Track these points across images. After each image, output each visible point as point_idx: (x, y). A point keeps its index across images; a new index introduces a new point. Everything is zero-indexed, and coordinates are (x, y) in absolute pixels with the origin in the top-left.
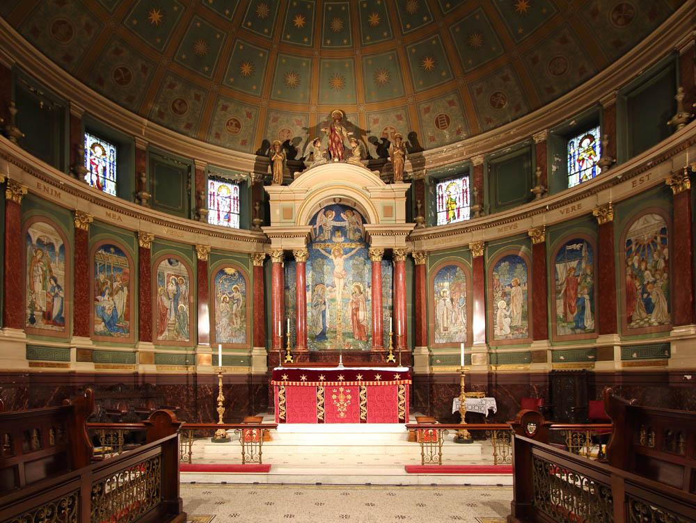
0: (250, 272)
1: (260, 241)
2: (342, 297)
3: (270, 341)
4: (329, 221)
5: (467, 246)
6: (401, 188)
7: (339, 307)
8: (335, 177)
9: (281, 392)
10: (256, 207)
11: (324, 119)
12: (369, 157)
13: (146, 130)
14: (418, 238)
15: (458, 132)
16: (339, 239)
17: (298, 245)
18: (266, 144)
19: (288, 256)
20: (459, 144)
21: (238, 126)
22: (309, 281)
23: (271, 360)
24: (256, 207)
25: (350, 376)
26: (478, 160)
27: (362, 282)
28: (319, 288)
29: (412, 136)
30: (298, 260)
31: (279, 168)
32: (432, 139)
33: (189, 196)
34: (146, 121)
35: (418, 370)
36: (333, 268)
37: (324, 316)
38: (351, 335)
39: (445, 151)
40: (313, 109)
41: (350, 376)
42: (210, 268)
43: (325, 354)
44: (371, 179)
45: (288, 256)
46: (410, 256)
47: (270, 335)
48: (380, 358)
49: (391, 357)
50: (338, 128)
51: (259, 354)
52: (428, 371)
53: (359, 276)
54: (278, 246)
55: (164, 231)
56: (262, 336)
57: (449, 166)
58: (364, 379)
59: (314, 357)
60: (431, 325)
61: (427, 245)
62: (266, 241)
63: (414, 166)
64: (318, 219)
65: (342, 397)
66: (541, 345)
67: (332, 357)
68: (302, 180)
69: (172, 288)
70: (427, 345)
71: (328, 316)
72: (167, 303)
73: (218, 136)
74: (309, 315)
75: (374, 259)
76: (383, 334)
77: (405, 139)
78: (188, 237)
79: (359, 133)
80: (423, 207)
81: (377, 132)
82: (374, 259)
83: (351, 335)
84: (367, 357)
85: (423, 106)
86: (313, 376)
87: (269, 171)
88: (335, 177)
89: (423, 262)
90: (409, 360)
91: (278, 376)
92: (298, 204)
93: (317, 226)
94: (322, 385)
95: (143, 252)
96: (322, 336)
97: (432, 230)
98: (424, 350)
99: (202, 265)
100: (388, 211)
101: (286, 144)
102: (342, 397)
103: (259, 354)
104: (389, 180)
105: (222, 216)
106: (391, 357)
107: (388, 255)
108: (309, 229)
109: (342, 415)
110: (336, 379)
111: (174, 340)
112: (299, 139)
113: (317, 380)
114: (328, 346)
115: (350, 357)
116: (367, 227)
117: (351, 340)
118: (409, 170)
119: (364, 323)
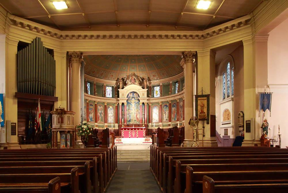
0: (115, 107)
1: (117, 100)
2: (134, 113)
3: (119, 122)
4: (131, 95)
5: (158, 102)
6: (146, 90)
7: (133, 114)
8: (133, 87)
9: (123, 132)
10: (116, 93)
11: (130, 74)
12: (140, 81)
13: (96, 80)
14: (150, 100)
15: (157, 78)
16: (133, 99)
17: (125, 102)
18: (118, 79)
19: (123, 104)
20: (158, 80)
21: (113, 76)
22: (127, 109)
23: (120, 126)
24: (116, 93)
25: (135, 129)
26: (161, 84)
27: (138, 109)
28: (129, 111)
29: (149, 78)
30: (125, 105)
31: (121, 86)
32: (153, 79)
33: (103, 91)
34: (96, 78)
35: (149, 128)
36: (132, 106)
37: (130, 116)
38: (136, 121)
39: (155, 81)
40: (128, 72)
41: (135, 129)
42: (107, 106)
43: (130, 125)
44: (140, 87)
45: (123, 104)
46: (148, 103)
47: (119, 120)
48: (141, 125)
49: (144, 125)
50: (133, 77)
51: (117, 125)
52: (151, 128)
53: (137, 108)
54: (121, 102)
55: (99, 100)
56: (117, 120)
57: (156, 84)
58: (137, 130)
59: (128, 125)
60: (152, 118)
61: (151, 101)
62: (118, 100)
63: (149, 83)
64: (129, 95)
65: (133, 133)
66: (170, 123)
67: (132, 125)
68: (126, 88)
69: (100, 112)
70: (151, 123)
71: (131, 116)
72: (100, 115)
73: (108, 78)
74: (127, 116)
75: (140, 105)
76: (142, 121)
77: (147, 78)
78: (103, 101)
79: (137, 77)
80: (151, 93)
81: (142, 76)
82: (140, 105)
83: (136, 121)
84: (139, 125)
85: (150, 73)
86: (128, 129)
87: (119, 84)
88: (133, 87)
89: (151, 105)
90: (147, 126)
91: (122, 129)
92: (125, 93)
93: (129, 97)
94: (130, 131)
95: (96, 105)
96: (130, 121)
97: (152, 98)
98: (150, 124)
99: (105, 106)
100: (143, 94)
101: (122, 79)
102: (133, 133)
103: (117, 125)
104: (143, 88)
105: (108, 94)
106: (144, 125)
107: (143, 103)
108: (127, 98)
109: (134, 136)
110: (133, 130)
111: (100, 122)
112: (125, 77)
113: (129, 130)
114: (131, 123)
115: (135, 125)
116: (139, 98)
117: (135, 122)
118: (148, 84)
119: (138, 118)
